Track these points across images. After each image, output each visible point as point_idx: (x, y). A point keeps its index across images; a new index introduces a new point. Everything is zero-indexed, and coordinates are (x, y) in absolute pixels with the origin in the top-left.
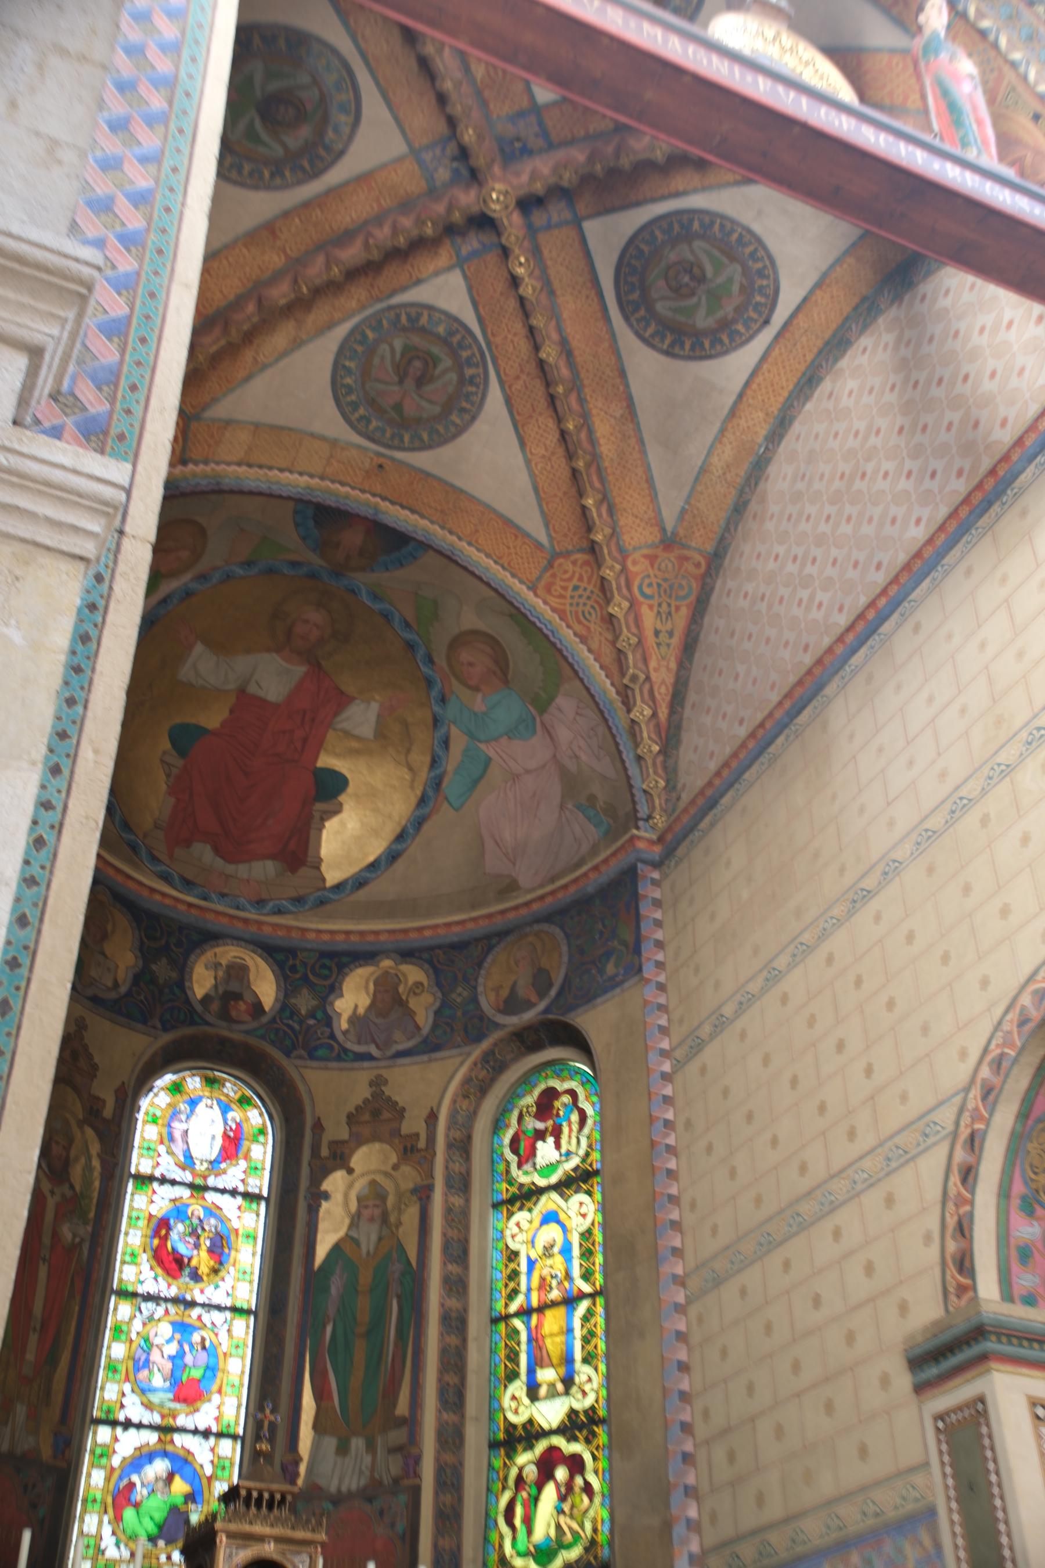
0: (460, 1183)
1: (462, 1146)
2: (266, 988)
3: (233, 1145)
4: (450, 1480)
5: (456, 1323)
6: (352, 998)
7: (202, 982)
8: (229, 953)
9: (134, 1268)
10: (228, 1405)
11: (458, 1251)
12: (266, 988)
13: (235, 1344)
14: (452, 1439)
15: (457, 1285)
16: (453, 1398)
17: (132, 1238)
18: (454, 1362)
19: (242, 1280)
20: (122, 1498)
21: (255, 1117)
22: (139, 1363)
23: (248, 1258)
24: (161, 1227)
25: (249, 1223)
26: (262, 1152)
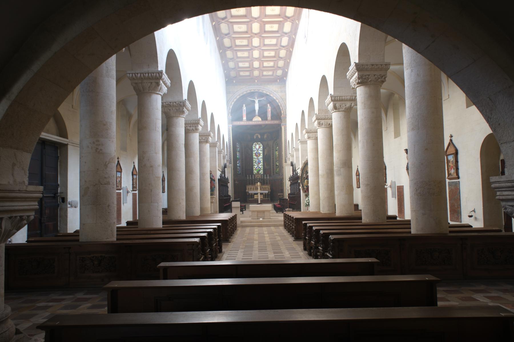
0: (273, 150)
1: (273, 147)
2: (259, 137)
3: (260, 147)
4: (273, 168)
5: (273, 159)
6: (265, 137)
7: (255, 137)
8: (256, 135)
9: (255, 157)
10: (262, 164)
11: (273, 154)
12: (259, 137)
13: (261, 160)
14: (273, 165)
15: (273, 156)
16: (273, 163)
17: (254, 155)
18: (273, 161)
19: (261, 156)
20: (256, 170)
21: (261, 145)
22: (256, 162)
23: (262, 155)
24: (255, 154)
25: (262, 152)
26: (262, 147)
